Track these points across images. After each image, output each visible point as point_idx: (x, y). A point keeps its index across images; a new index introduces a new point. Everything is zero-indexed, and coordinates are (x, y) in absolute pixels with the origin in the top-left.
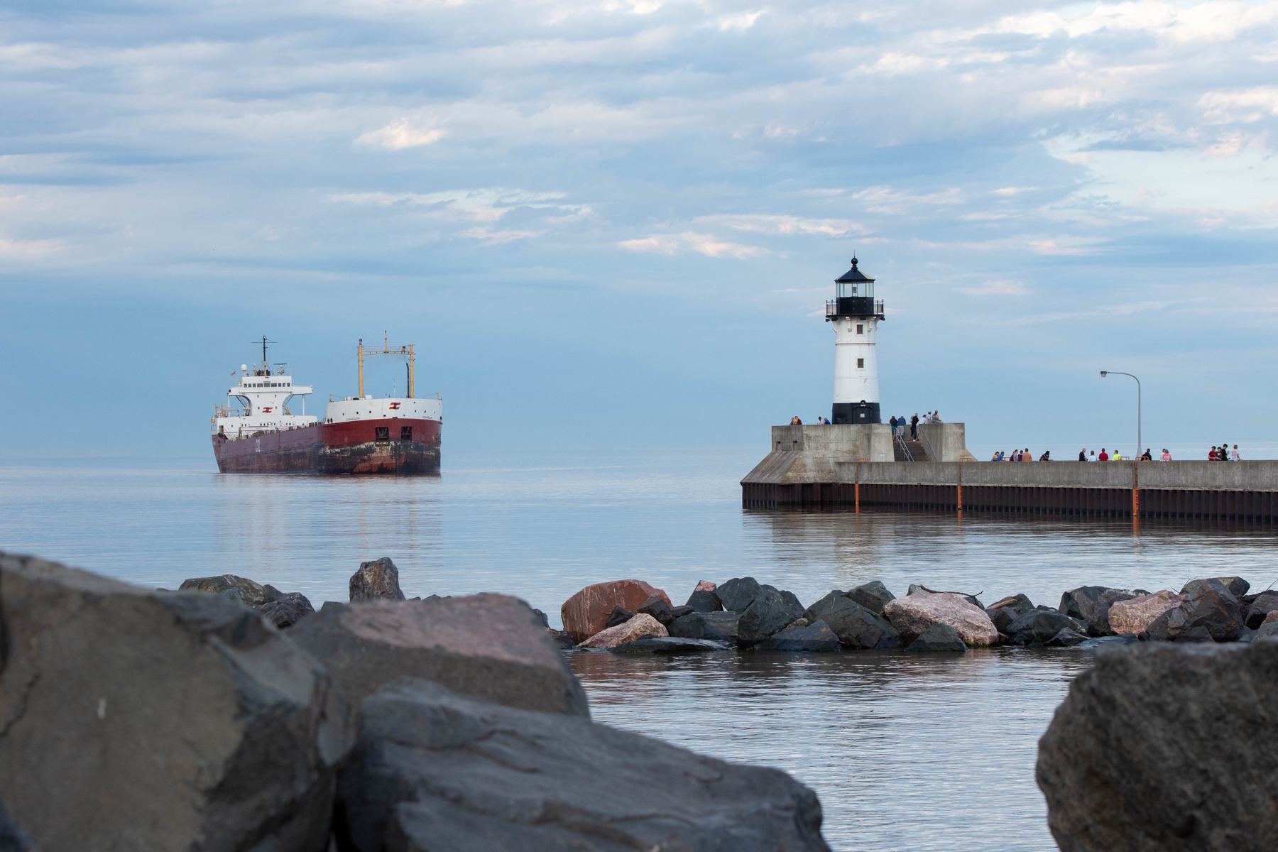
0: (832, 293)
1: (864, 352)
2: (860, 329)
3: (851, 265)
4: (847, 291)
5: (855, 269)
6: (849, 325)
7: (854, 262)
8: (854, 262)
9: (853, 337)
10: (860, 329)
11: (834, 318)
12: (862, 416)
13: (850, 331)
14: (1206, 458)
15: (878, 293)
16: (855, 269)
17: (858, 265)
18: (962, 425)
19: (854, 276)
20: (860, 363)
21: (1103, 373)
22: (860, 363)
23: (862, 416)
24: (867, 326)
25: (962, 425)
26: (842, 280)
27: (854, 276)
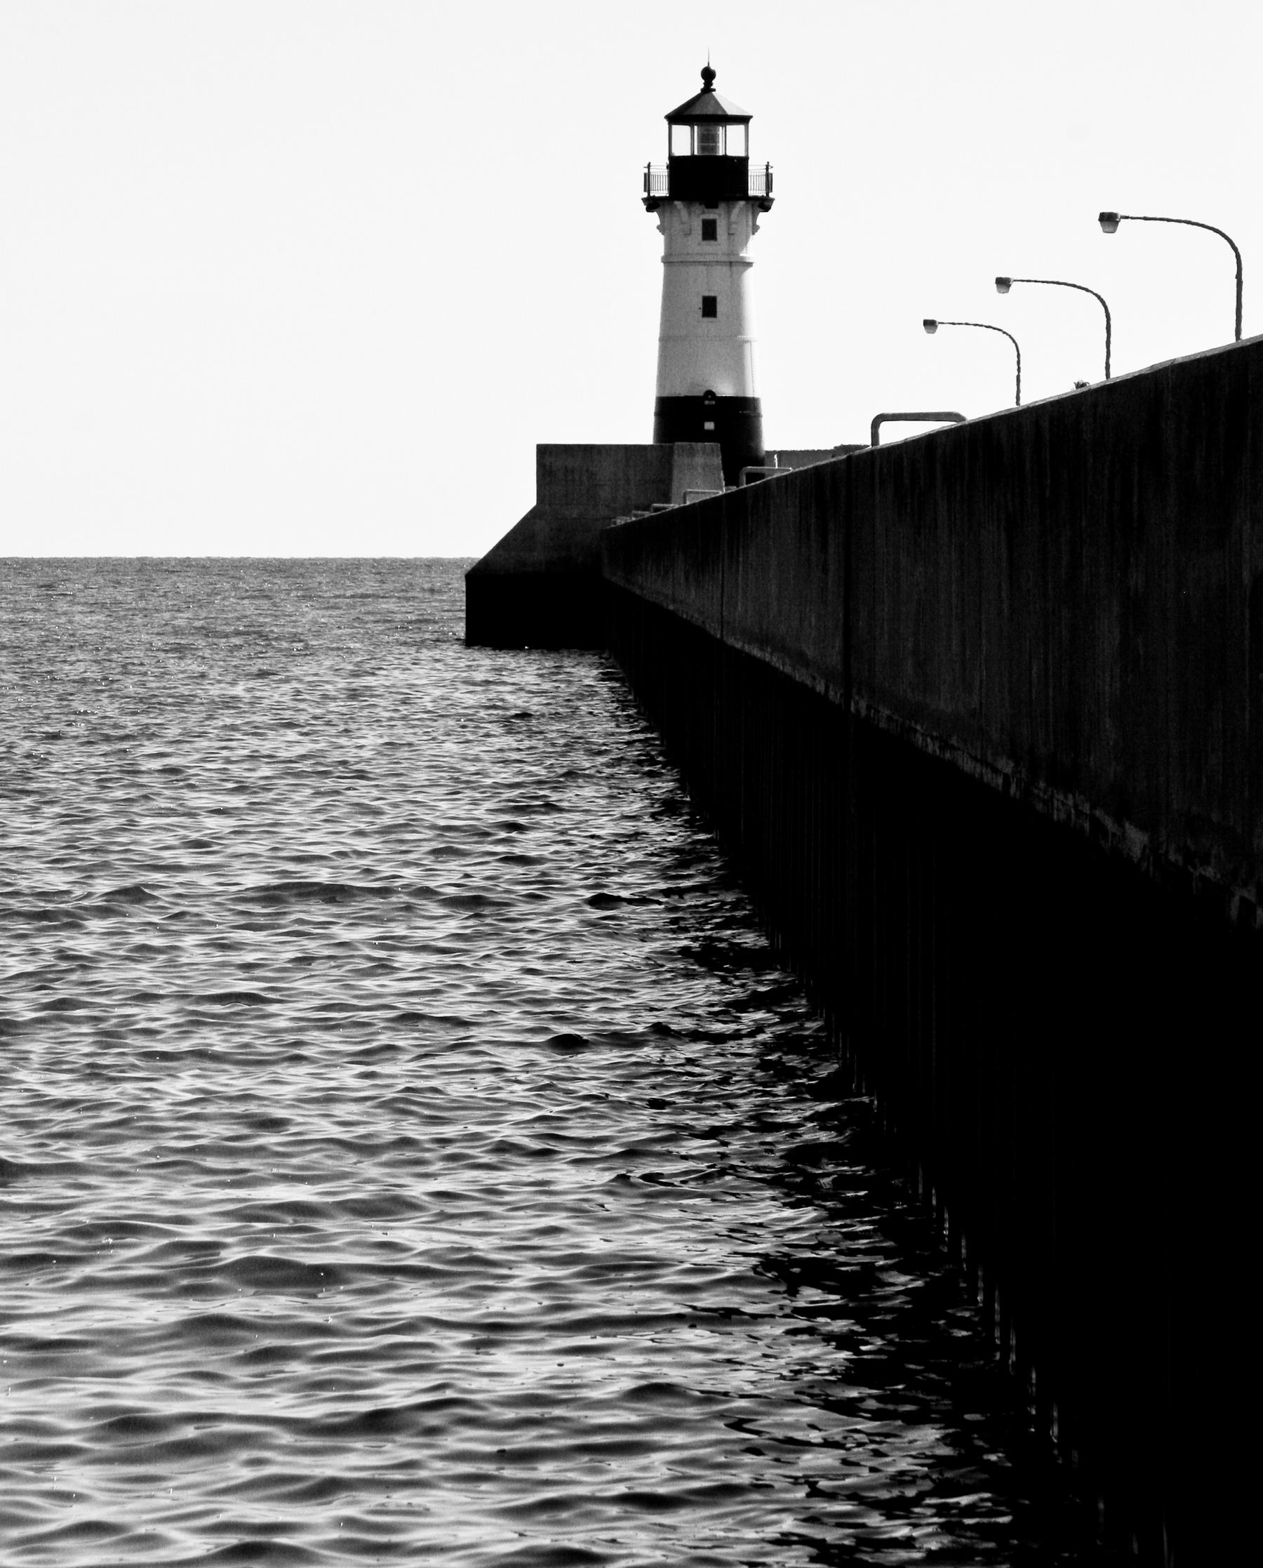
0: (659, 146)
2: (709, 231)
3: (700, 84)
4: (685, 141)
6: (693, 218)
7: (708, 75)
8: (708, 75)
10: (709, 231)
11: (652, 204)
12: (709, 426)
13: (688, 233)
17: (716, 83)
23: (709, 426)
26: (675, 118)
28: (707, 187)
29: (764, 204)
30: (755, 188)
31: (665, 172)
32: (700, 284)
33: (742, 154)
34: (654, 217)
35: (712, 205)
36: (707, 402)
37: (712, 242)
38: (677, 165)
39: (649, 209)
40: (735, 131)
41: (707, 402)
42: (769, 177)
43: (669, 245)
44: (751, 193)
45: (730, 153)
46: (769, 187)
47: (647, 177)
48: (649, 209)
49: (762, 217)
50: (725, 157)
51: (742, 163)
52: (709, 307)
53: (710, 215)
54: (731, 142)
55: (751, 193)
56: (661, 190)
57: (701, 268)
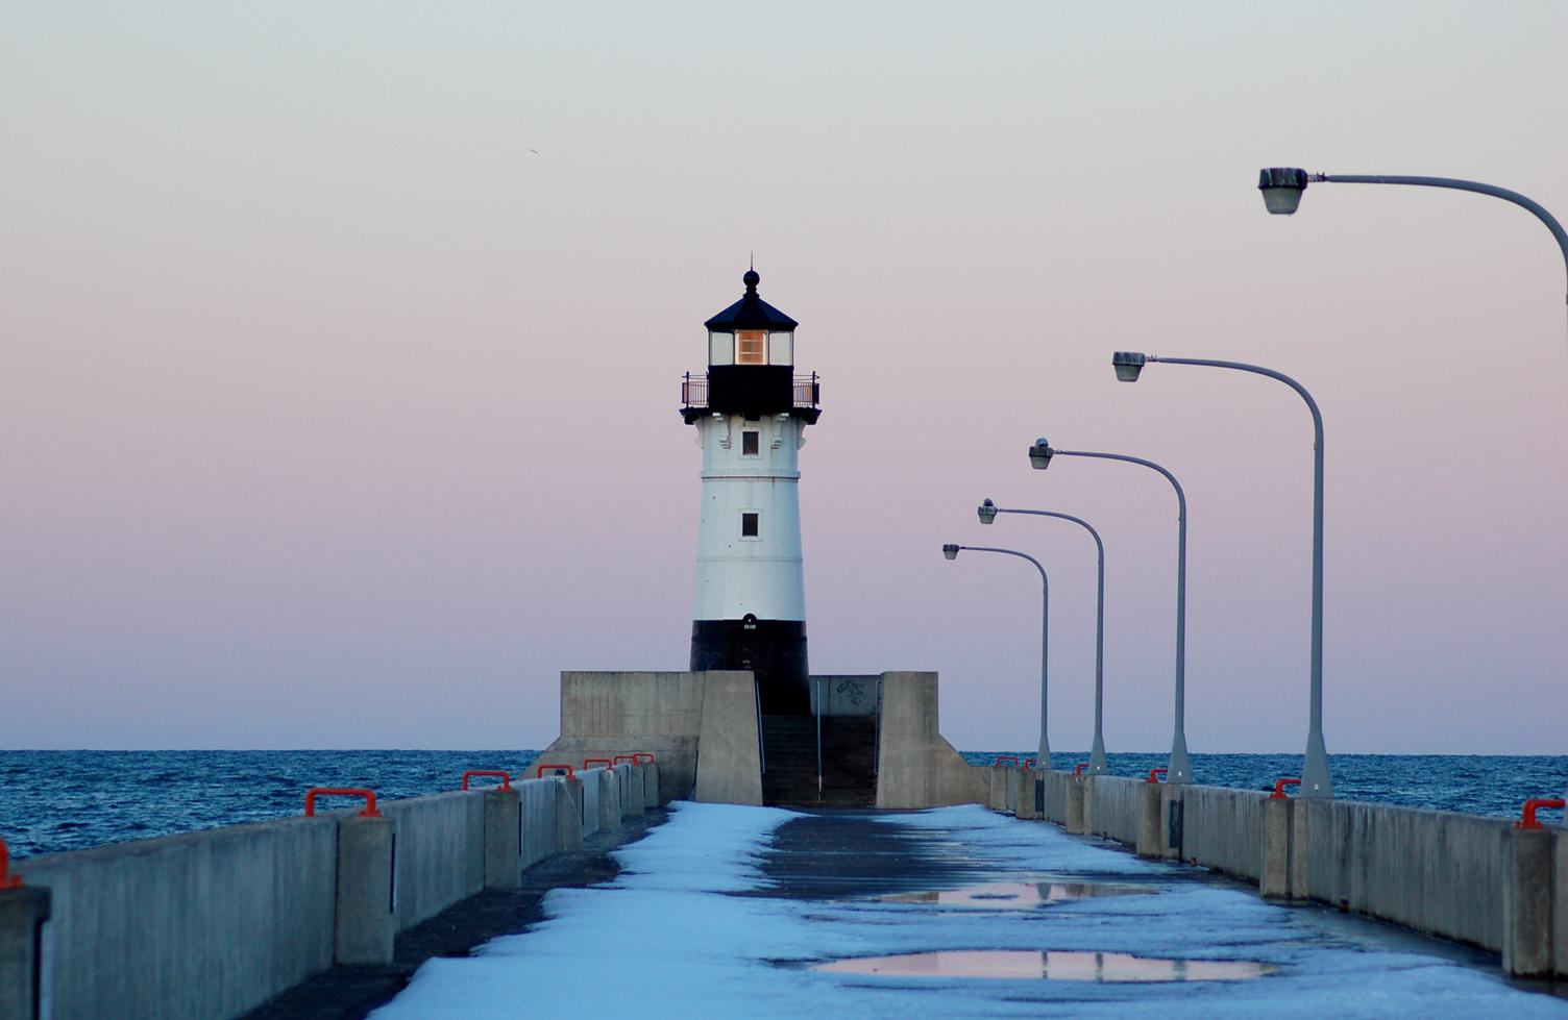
1: (759, 500)
3: (743, 289)
4: (728, 350)
5: (751, 296)
6: (730, 431)
7: (752, 279)
8: (752, 279)
9: (734, 459)
10: (751, 444)
11: (691, 415)
16: (751, 296)
18: (933, 675)
19: (751, 314)
20: (750, 525)
22: (750, 525)
24: (768, 433)
25: (933, 675)
26: (715, 325)
27: (751, 314)
28: (752, 394)
29: (811, 416)
30: (800, 401)
31: (705, 382)
33: (787, 363)
34: (693, 428)
35: (752, 416)
36: (746, 627)
37: (754, 456)
38: (717, 374)
39: (689, 421)
40: (779, 339)
41: (746, 627)
42: (815, 388)
44: (796, 404)
45: (771, 363)
46: (816, 399)
47: (686, 386)
48: (689, 421)
49: (808, 428)
50: (769, 367)
51: (786, 372)
53: (751, 428)
54: (774, 350)
55: (796, 404)
56: (700, 399)
57: (743, 484)
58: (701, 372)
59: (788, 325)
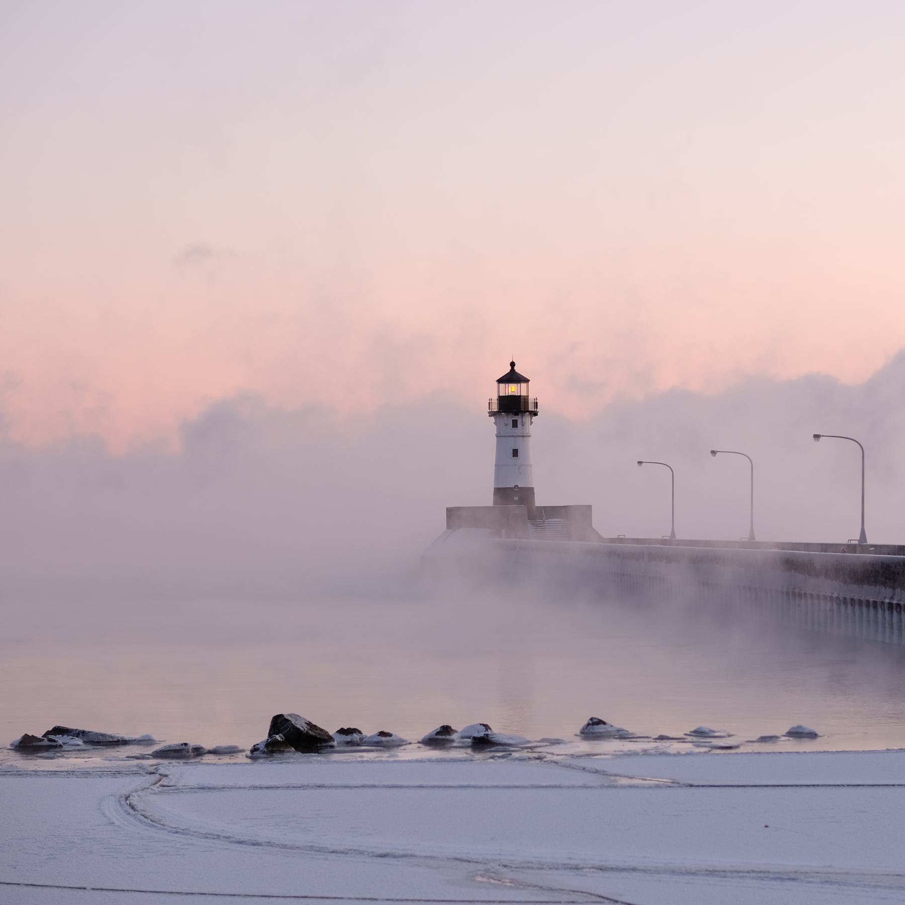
0: (492, 392)
2: (515, 424)
5: (513, 370)
6: (508, 419)
7: (513, 364)
8: (513, 364)
10: (515, 424)
11: (492, 414)
12: (516, 498)
14: (487, 499)
15: (532, 391)
16: (513, 370)
17: (516, 368)
18: (590, 506)
19: (512, 377)
21: (640, 463)
25: (590, 506)
26: (500, 381)
27: (512, 377)
29: (536, 414)
30: (531, 408)
32: (512, 444)
35: (516, 414)
40: (524, 385)
42: (536, 404)
43: (498, 430)
49: (534, 418)
52: (515, 453)
53: (515, 418)
56: (495, 408)
58: (495, 398)
59: (527, 381)
